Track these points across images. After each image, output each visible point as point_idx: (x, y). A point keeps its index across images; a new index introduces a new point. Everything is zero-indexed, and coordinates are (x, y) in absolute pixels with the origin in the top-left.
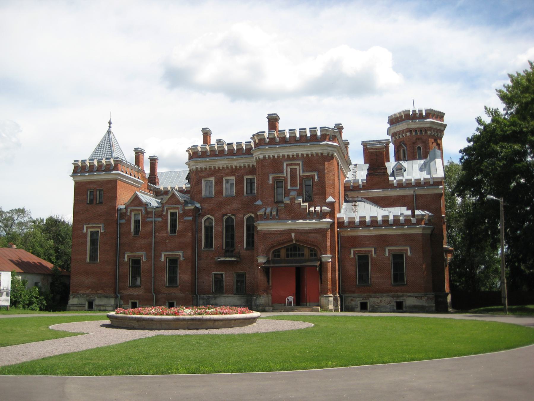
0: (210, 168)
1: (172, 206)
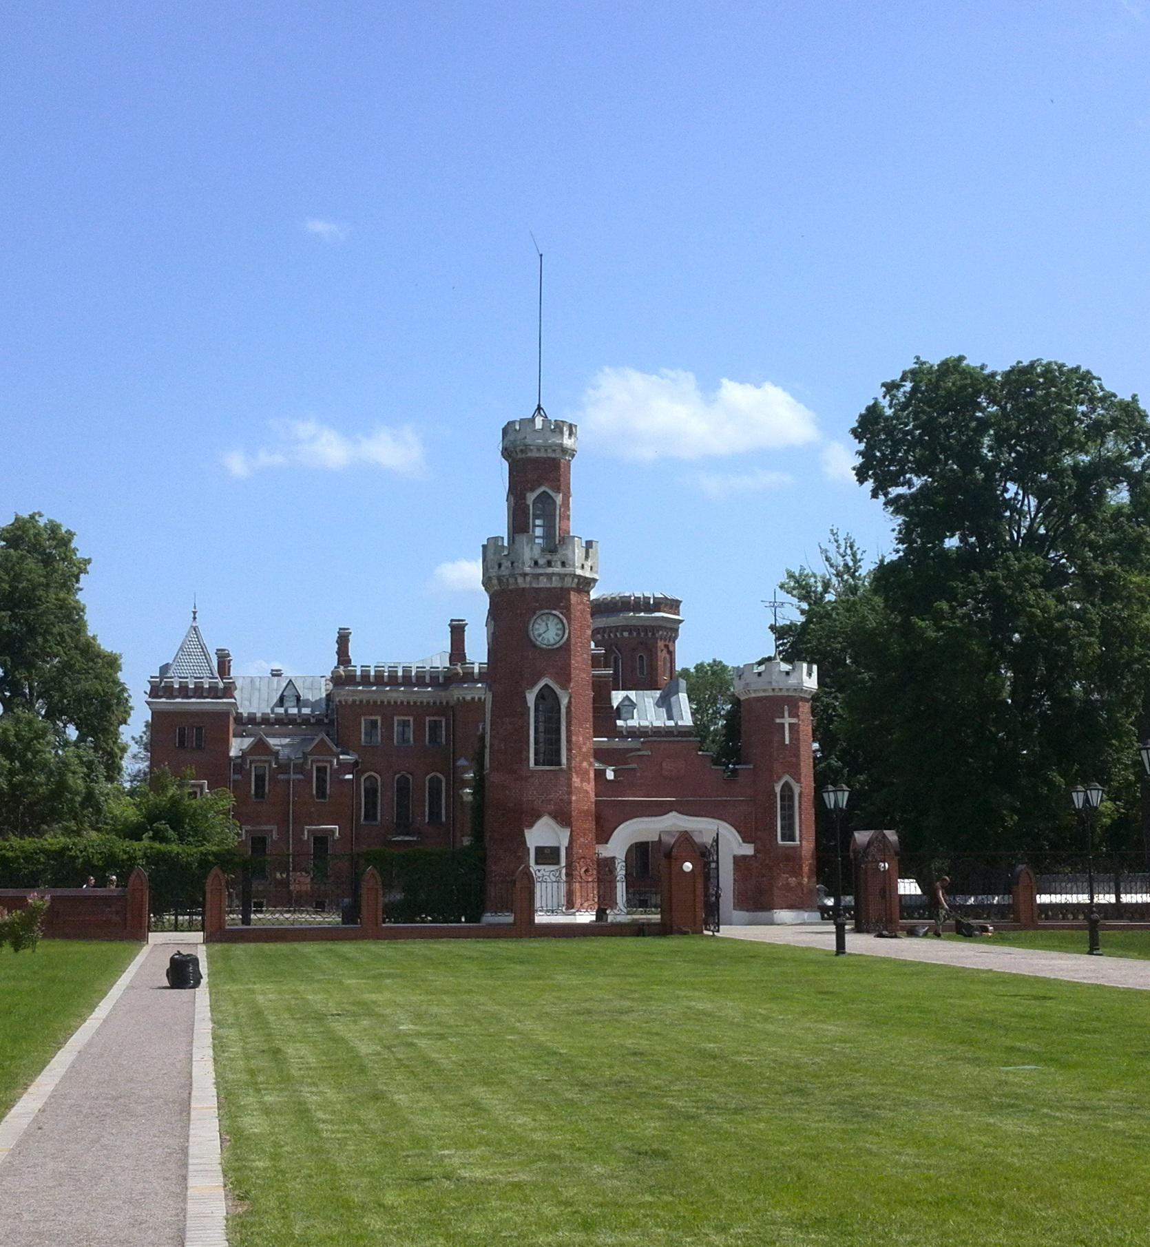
0: (375, 702)
1: (321, 758)
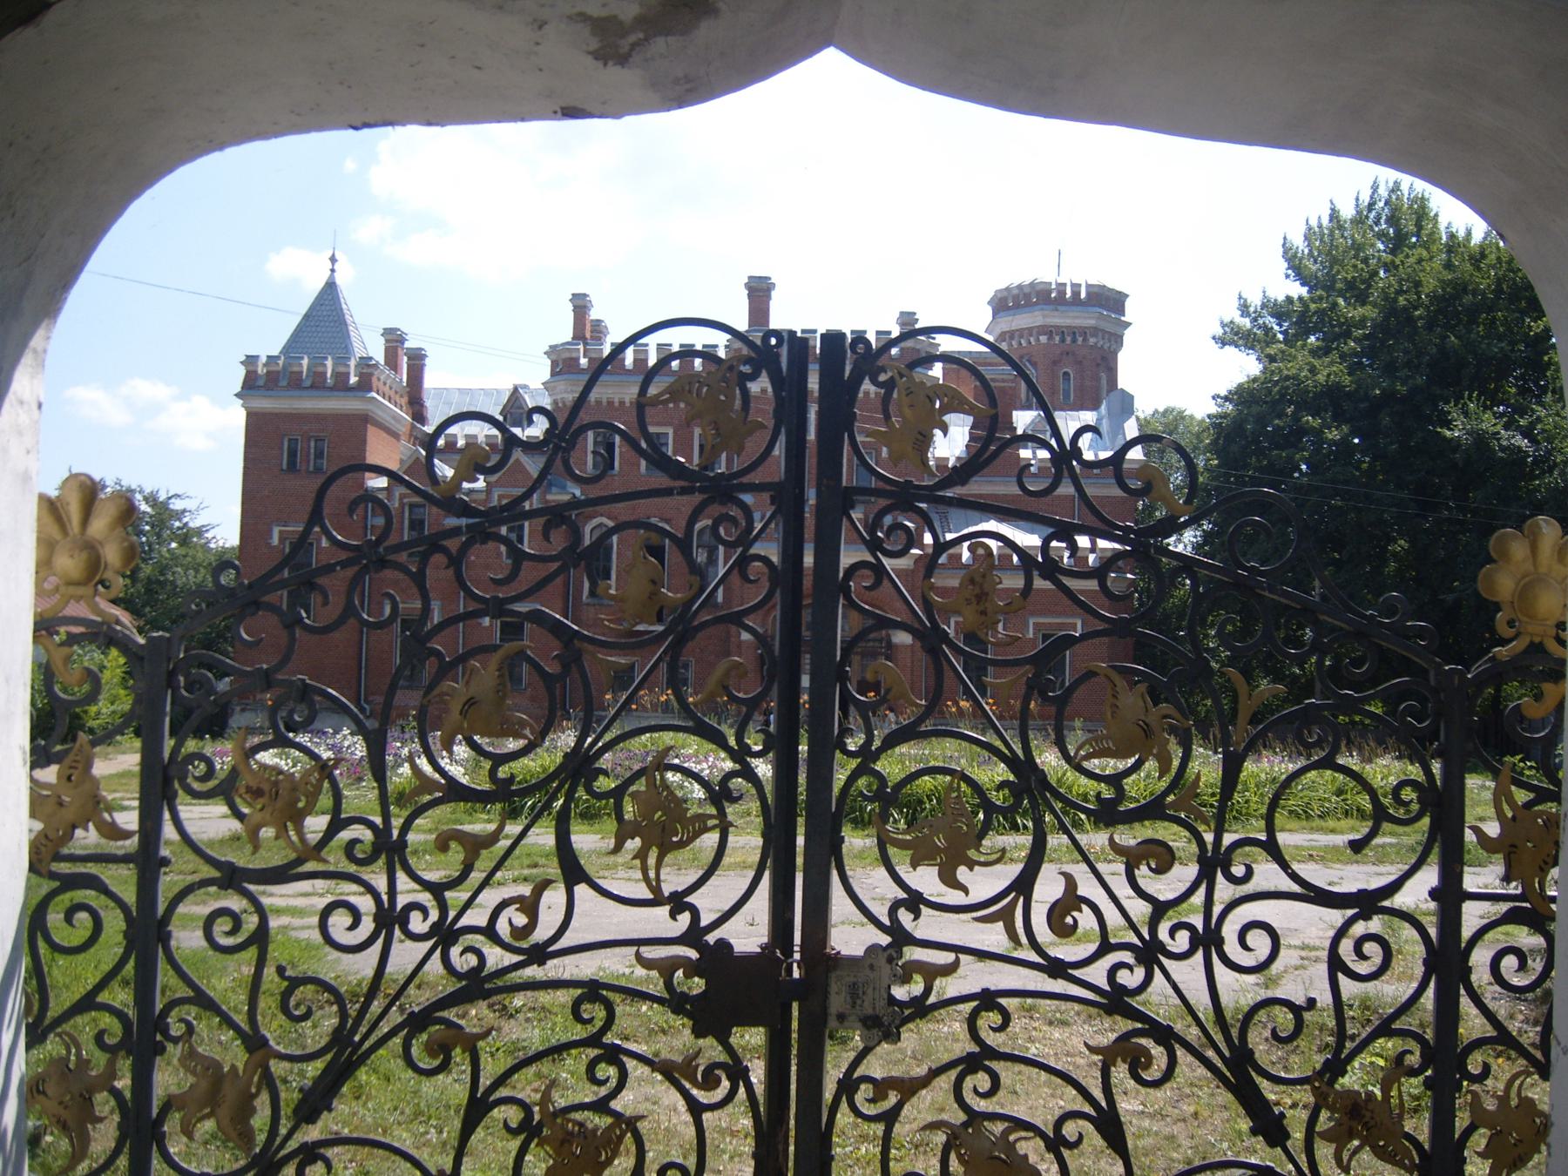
0: (610, 403)
